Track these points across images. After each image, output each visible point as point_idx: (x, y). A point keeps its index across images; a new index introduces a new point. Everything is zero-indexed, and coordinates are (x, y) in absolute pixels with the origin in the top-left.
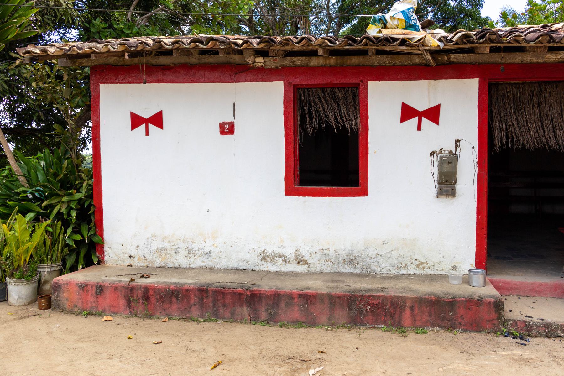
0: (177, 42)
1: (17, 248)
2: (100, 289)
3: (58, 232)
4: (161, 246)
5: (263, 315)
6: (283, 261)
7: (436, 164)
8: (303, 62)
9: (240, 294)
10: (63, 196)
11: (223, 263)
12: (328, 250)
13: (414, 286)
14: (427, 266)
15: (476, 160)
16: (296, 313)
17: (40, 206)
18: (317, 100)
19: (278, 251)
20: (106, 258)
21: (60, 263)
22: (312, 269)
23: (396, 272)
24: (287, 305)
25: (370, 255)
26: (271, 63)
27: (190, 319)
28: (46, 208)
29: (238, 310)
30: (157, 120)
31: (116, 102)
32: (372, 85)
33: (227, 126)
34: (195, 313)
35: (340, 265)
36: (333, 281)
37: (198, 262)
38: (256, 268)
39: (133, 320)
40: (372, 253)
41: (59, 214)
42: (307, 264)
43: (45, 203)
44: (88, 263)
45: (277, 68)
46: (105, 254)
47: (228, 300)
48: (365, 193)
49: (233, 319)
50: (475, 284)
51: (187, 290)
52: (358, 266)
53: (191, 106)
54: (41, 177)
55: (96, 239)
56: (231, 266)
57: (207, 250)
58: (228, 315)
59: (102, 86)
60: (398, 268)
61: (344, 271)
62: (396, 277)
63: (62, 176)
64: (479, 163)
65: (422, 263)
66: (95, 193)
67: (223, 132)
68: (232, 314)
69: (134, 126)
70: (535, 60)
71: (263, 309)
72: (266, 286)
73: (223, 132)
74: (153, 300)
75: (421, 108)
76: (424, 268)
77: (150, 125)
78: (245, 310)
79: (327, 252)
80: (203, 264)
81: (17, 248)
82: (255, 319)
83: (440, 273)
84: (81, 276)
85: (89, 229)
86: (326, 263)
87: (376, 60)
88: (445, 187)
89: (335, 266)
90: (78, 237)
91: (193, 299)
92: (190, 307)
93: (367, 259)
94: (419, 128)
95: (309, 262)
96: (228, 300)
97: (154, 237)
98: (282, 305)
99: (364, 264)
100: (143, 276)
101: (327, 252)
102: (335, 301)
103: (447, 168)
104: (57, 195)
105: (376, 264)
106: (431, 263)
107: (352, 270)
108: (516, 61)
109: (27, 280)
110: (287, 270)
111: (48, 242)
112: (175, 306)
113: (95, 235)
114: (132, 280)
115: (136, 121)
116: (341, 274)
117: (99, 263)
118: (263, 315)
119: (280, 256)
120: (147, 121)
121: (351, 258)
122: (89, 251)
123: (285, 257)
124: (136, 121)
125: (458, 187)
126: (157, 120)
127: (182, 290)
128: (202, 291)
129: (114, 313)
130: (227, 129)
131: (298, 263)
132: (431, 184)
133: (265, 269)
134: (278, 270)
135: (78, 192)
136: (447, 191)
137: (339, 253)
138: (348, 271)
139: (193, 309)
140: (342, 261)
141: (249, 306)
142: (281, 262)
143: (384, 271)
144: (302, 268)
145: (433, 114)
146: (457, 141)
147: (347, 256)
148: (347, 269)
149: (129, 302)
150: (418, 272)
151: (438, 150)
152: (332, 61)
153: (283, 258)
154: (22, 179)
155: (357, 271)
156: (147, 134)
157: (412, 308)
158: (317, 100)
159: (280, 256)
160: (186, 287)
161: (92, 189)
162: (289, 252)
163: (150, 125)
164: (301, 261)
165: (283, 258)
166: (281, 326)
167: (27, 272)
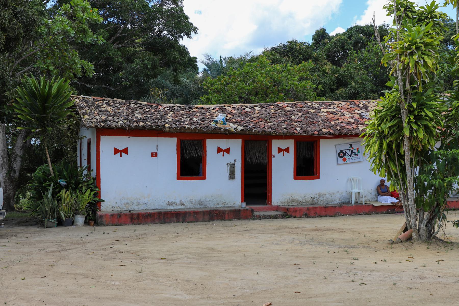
5: (181, 220)
19: (174, 201)
23: (216, 206)
27: (155, 224)
32: (208, 140)
34: (156, 221)
40: (207, 200)
49: (171, 222)
51: (154, 213)
53: (139, 146)
56: (155, 208)
74: (141, 218)
78: (175, 219)
88: (232, 176)
97: (123, 198)
98: (187, 216)
103: (232, 169)
107: (201, 207)
112: (149, 220)
115: (116, 151)
118: (181, 220)
124: (116, 151)
125: (236, 176)
126: (125, 151)
128: (160, 213)
130: (154, 155)
144: (183, 207)
145: (228, 151)
146: (235, 160)
150: (223, 206)
155: (203, 207)
156: (121, 156)
157: (228, 214)
162: (178, 201)
164: (182, 204)
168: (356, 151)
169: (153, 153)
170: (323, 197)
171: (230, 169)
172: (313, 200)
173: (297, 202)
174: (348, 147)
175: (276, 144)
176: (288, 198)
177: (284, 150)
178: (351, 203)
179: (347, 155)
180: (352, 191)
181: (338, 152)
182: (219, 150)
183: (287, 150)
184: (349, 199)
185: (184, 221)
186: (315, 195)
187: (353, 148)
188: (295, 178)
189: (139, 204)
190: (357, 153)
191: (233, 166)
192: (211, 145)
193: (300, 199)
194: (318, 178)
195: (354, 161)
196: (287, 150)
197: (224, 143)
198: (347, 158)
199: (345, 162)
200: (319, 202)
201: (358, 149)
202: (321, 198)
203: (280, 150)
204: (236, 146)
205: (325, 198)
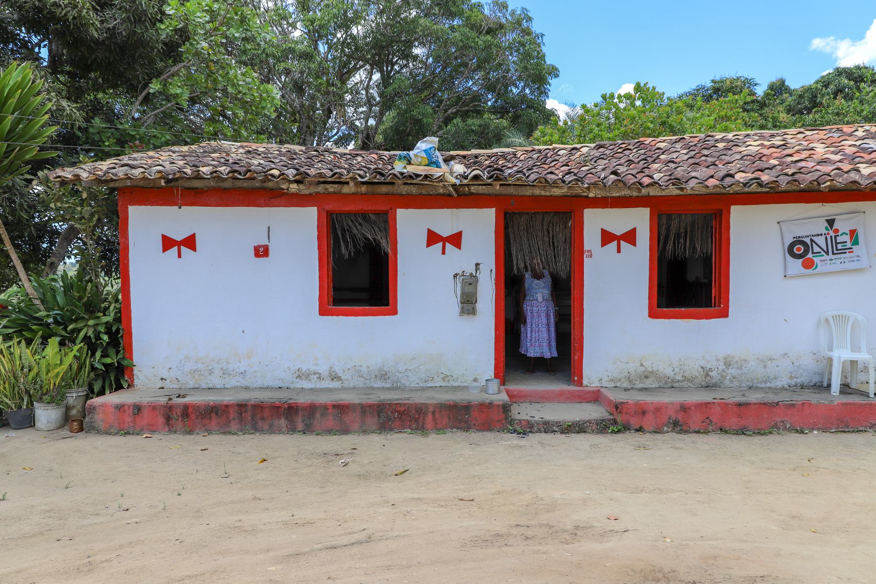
0: (215, 172)
1: (48, 372)
2: (138, 409)
3: (84, 356)
4: (194, 368)
5: (300, 426)
7: (459, 285)
9: (278, 407)
10: (88, 320)
11: (259, 383)
13: (437, 396)
14: (451, 379)
15: (494, 282)
16: (330, 421)
17: (65, 329)
18: (350, 223)
19: (313, 368)
20: (136, 381)
21: (86, 388)
22: (346, 385)
23: (424, 385)
24: (322, 415)
26: (304, 189)
28: (73, 331)
29: (276, 422)
30: (190, 242)
31: (145, 224)
32: (400, 212)
33: (262, 249)
34: (234, 427)
36: (364, 394)
37: (233, 382)
38: (292, 386)
39: (173, 436)
40: (402, 368)
41: (86, 338)
43: (70, 327)
44: (119, 387)
46: (135, 377)
47: (267, 413)
48: (394, 312)
49: (272, 430)
50: (490, 392)
51: (227, 406)
53: (223, 228)
54: (60, 299)
55: (125, 363)
56: (266, 385)
57: (242, 370)
58: (266, 427)
59: (131, 209)
60: (426, 382)
61: (376, 385)
62: (423, 389)
63: (86, 299)
65: (447, 376)
66: (123, 315)
67: (257, 255)
68: (271, 426)
69: (165, 249)
70: (543, 193)
71: (300, 420)
72: (302, 400)
73: (257, 255)
74: (193, 416)
77: (182, 247)
78: (283, 422)
80: (239, 384)
81: (48, 372)
82: (292, 429)
83: (463, 385)
84: (112, 398)
85: (117, 353)
87: (405, 190)
88: (466, 306)
89: (367, 382)
90: (108, 361)
91: (232, 414)
92: (230, 422)
94: (443, 253)
96: (267, 413)
98: (318, 415)
100: (179, 396)
102: (365, 409)
103: (468, 289)
104: (83, 318)
106: (455, 376)
107: (383, 385)
108: (528, 194)
109: (58, 404)
111: (75, 367)
112: (214, 422)
113: (123, 358)
114: (170, 399)
115: (168, 243)
116: (373, 388)
117: (129, 386)
118: (300, 426)
119: (315, 374)
120: (179, 244)
122: (118, 375)
124: (168, 243)
125: (478, 306)
126: (190, 242)
127: (221, 406)
128: (242, 407)
129: (153, 431)
130: (262, 252)
132: (454, 304)
135: (105, 315)
136: (468, 310)
139: (233, 423)
141: (287, 418)
143: (413, 385)
144: (336, 384)
145: (456, 240)
148: (379, 384)
149: (168, 419)
150: (443, 384)
151: (460, 273)
152: (364, 189)
154: (37, 302)
155: (388, 385)
159: (315, 374)
160: (225, 403)
161: (120, 312)
162: (323, 369)
163: (182, 247)
164: (335, 377)
166: (317, 435)
167: (56, 397)
168: (847, 238)
169: (259, 246)
170: (740, 368)
171: (463, 288)
174: (821, 226)
175: (594, 221)
176: (633, 367)
177: (618, 238)
181: (789, 240)
182: (433, 238)
183: (630, 237)
184: (822, 374)
185: (308, 430)
188: (653, 315)
190: (849, 245)
191: (471, 281)
192: (411, 225)
193: (669, 372)
195: (838, 267)
196: (630, 237)
197: (444, 220)
198: (817, 260)
199: (810, 271)
200: (727, 382)
201: (853, 233)
202: (733, 371)
203: (607, 237)
204: (480, 227)
205: (745, 371)
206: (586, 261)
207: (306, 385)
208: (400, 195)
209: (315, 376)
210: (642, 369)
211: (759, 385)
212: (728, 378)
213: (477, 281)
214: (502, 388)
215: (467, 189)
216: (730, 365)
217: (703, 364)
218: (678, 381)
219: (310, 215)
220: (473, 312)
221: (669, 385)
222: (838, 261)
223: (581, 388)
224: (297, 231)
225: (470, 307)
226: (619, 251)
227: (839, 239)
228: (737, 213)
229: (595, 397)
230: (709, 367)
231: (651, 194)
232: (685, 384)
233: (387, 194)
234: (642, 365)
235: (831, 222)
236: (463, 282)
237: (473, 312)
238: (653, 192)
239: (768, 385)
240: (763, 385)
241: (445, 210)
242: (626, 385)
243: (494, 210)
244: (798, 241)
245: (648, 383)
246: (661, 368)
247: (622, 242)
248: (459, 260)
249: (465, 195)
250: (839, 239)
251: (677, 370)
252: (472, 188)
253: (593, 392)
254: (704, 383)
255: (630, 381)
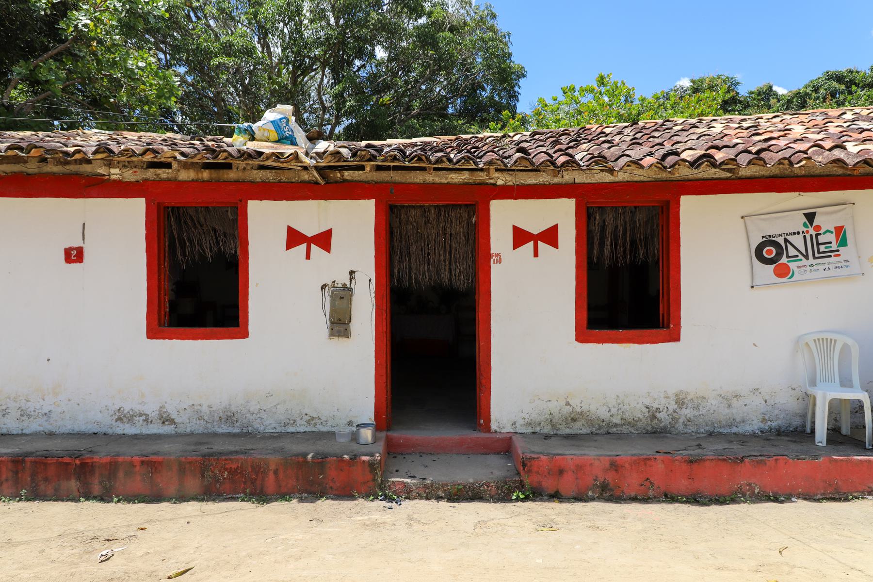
6: (144, 421)
7: (328, 299)
8: (170, 176)
11: (68, 426)
12: (200, 405)
15: (373, 295)
18: (189, 221)
19: (138, 408)
22: (181, 430)
23: (283, 430)
25: (251, 410)
26: (129, 176)
33: (74, 253)
35: (215, 423)
38: (110, 431)
40: (254, 407)
42: (175, 423)
45: (137, 181)
52: (238, 424)
56: (77, 429)
57: (47, 411)
60: (285, 425)
61: (220, 431)
64: (376, 298)
65: (313, 418)
75: (310, 233)
76: (315, 424)
79: (199, 407)
80: (41, 429)
86: (198, 422)
88: (336, 328)
89: (209, 425)
93: (248, 415)
94: (308, 257)
95: (176, 421)
99: (245, 421)
101: (199, 407)
105: (259, 421)
106: (323, 419)
110: (149, 432)
116: (215, 435)
119: (141, 415)
121: (229, 414)
123: (147, 415)
125: (354, 326)
130: (74, 255)
131: (163, 423)
132: (322, 323)
133: (121, 432)
134: (138, 432)
137: (214, 409)
138: (225, 431)
140: (217, 419)
142: (141, 422)
143: (269, 430)
144: (168, 429)
145: (324, 240)
147: (224, 412)
148: (224, 429)
150: (308, 429)
151: (330, 283)
152: (206, 175)
153: (144, 417)
155: (236, 431)
158: (189, 221)
159: (141, 415)
162: (151, 409)
164: (166, 420)
165: (144, 417)
168: (831, 237)
169: (71, 249)
170: (697, 408)
172: (654, 417)
173: (590, 422)
174: (798, 222)
175: (504, 216)
176: (556, 407)
177: (536, 238)
178: (813, 431)
179: (792, 252)
180: (811, 391)
181: (757, 240)
182: (294, 238)
183: (551, 236)
186: (663, 401)
187: (818, 228)
188: (581, 337)
189: (24, 414)
190: (834, 246)
191: (342, 293)
192: (267, 221)
193: (603, 413)
194: (677, 338)
196: (551, 236)
197: (310, 216)
198: (793, 266)
201: (839, 230)
203: (520, 237)
204: (355, 224)
205: (704, 412)
206: (495, 268)
207: (128, 429)
208: (252, 183)
209: (141, 418)
210: (568, 409)
211: (722, 431)
212: (681, 421)
213: (352, 295)
214: (383, 434)
215: (339, 175)
216: (683, 404)
217: (648, 402)
218: (616, 425)
219: (135, 210)
220: (346, 334)
221: (604, 430)
222: (822, 268)
223: (487, 435)
224: (120, 229)
225: (342, 328)
226: (536, 254)
227: (821, 239)
228: (688, 204)
229: (504, 447)
230: (655, 406)
231: (578, 181)
232: (625, 429)
233: (236, 182)
234: (568, 404)
235: (810, 217)
236: (332, 295)
237: (346, 334)
238: (580, 178)
239: (734, 430)
240: (727, 430)
241: (310, 202)
242: (547, 430)
243: (374, 200)
244: (769, 242)
245: (578, 428)
246: (593, 408)
247: (540, 244)
248: (329, 267)
249: (336, 182)
250: (821, 239)
251: (614, 411)
252: (346, 173)
253: (503, 440)
254: (649, 428)
255: (553, 426)
